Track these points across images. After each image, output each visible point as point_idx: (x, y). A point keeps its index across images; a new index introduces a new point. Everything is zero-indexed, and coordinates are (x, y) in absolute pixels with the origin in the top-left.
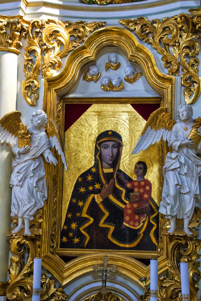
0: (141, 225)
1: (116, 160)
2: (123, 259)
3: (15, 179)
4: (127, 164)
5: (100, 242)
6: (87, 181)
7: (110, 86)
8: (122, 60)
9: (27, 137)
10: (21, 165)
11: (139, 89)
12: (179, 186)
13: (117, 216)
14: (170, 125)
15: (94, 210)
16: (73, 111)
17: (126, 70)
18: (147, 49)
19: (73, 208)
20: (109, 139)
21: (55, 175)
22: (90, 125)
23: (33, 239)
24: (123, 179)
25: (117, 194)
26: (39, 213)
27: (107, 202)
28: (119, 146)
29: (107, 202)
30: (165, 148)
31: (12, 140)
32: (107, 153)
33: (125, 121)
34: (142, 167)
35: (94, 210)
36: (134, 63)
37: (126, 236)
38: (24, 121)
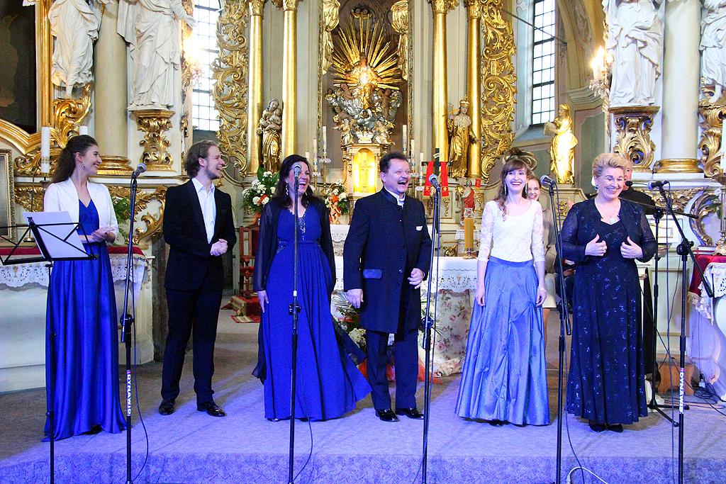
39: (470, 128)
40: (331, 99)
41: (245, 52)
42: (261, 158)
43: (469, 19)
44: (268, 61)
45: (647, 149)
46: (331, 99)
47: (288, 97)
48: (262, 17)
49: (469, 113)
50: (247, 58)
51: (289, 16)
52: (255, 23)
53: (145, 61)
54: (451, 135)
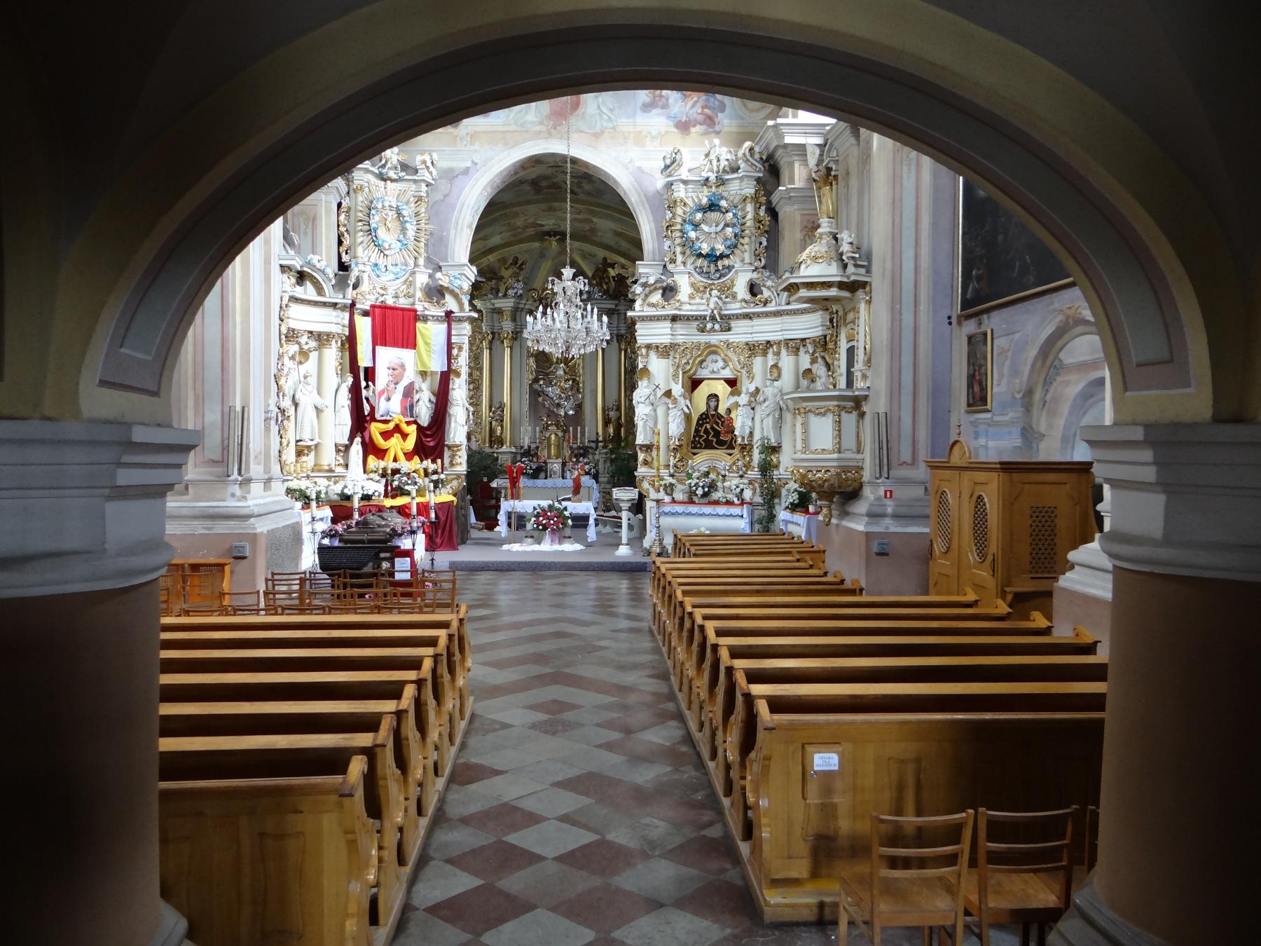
0: (727, 438)
1: (716, 408)
2: (720, 453)
3: (670, 419)
4: (722, 410)
5: (709, 446)
6: (703, 418)
7: (713, 372)
8: (719, 359)
9: (675, 401)
10: (673, 413)
11: (727, 373)
12: (743, 423)
13: (717, 434)
14: (739, 394)
15: (706, 431)
16: (695, 384)
17: (721, 364)
18: (730, 354)
19: (697, 431)
20: (713, 397)
21: (688, 417)
22: (703, 391)
23: (680, 446)
24: (720, 417)
25: (717, 424)
26: (682, 435)
27: (712, 428)
28: (718, 401)
29: (712, 428)
30: (737, 405)
31: (668, 400)
32: (713, 404)
33: (721, 389)
34: (729, 411)
35: (706, 431)
36: (724, 361)
37: (721, 443)
38: (674, 393)
39: (620, 418)
40: (536, 386)
41: (481, 370)
42: (491, 436)
43: (620, 350)
44: (495, 374)
45: (649, 459)
46: (536, 386)
47: (506, 399)
48: (491, 349)
49: (619, 409)
50: (482, 373)
51: (507, 351)
52: (486, 353)
53: (453, 425)
54: (607, 422)
